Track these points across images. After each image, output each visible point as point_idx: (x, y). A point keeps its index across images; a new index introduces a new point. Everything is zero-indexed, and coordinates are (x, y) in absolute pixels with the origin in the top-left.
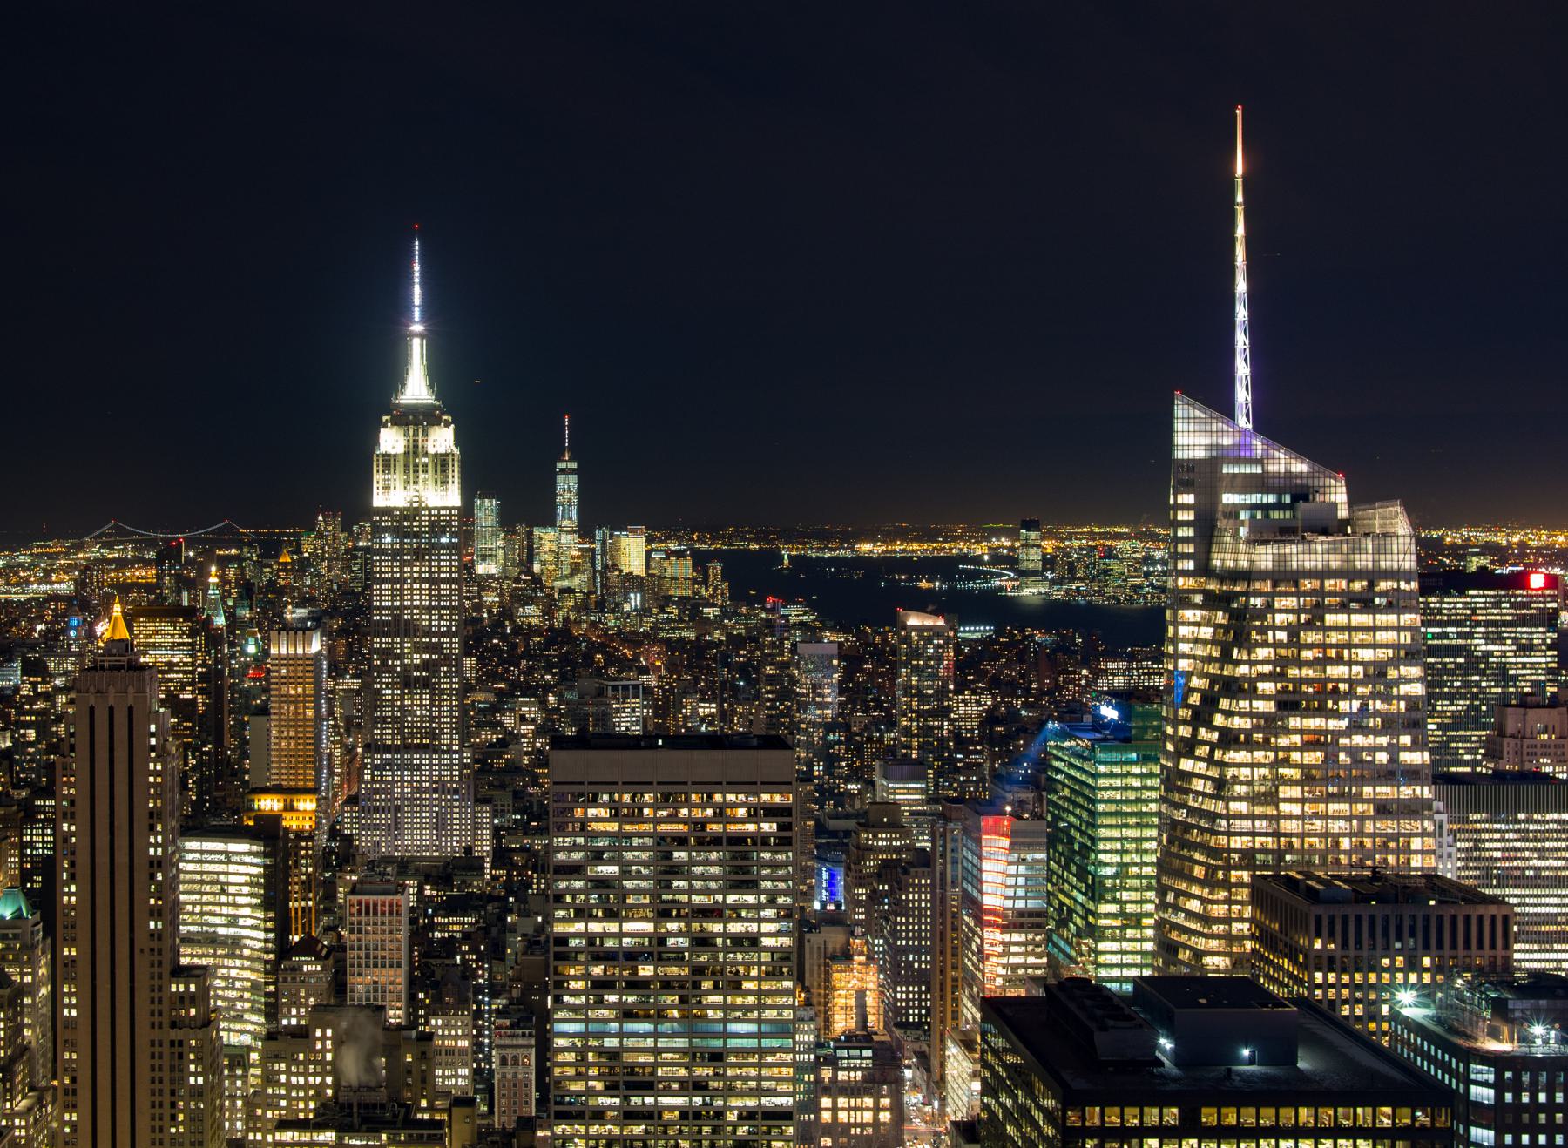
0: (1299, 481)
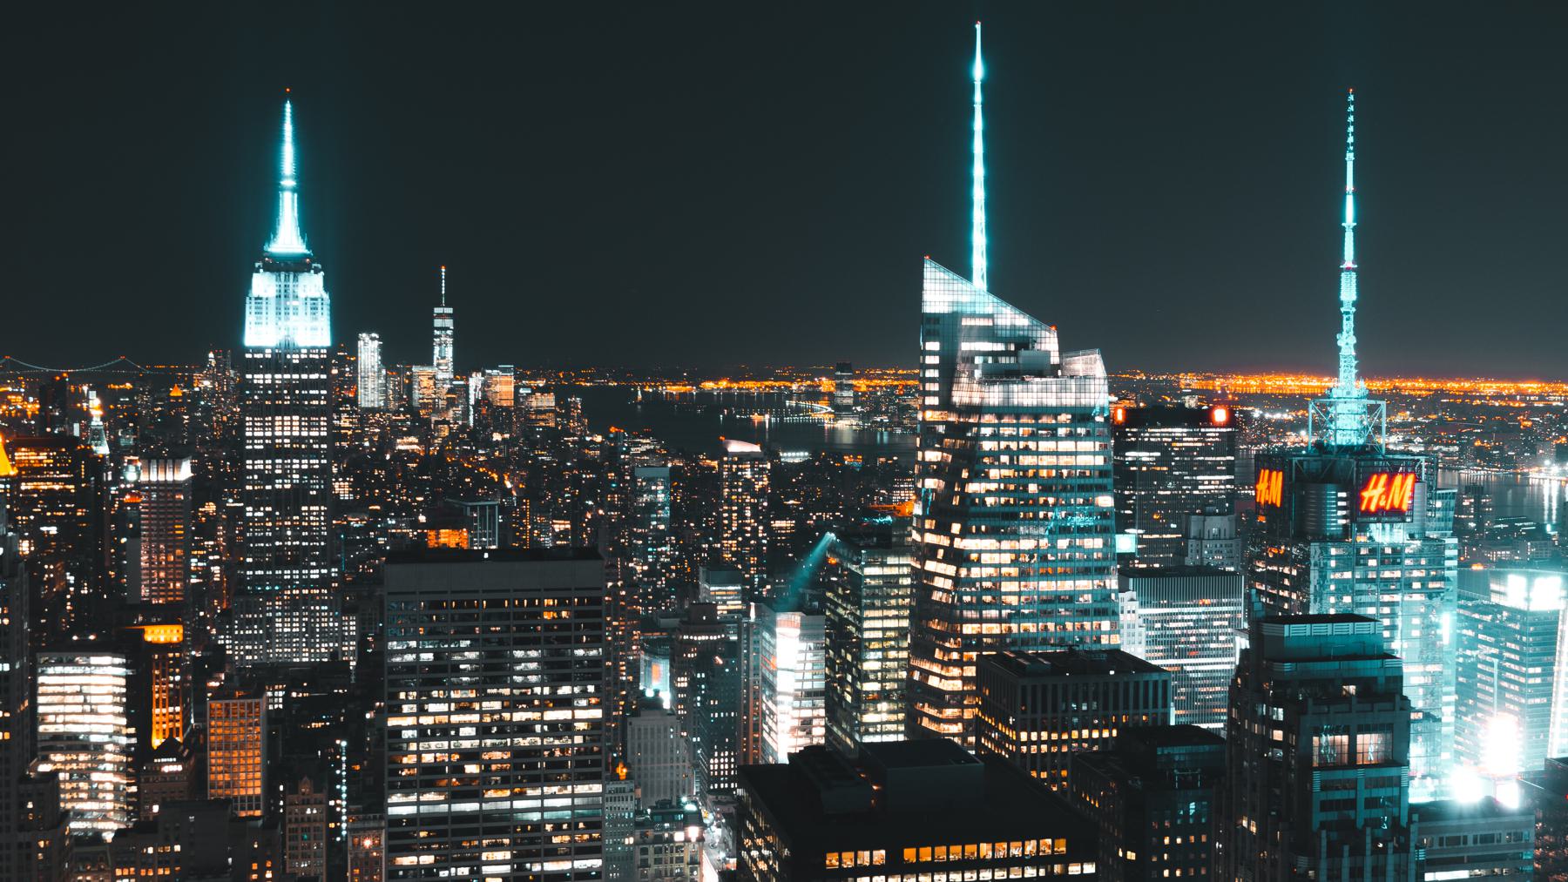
0: (1021, 333)
